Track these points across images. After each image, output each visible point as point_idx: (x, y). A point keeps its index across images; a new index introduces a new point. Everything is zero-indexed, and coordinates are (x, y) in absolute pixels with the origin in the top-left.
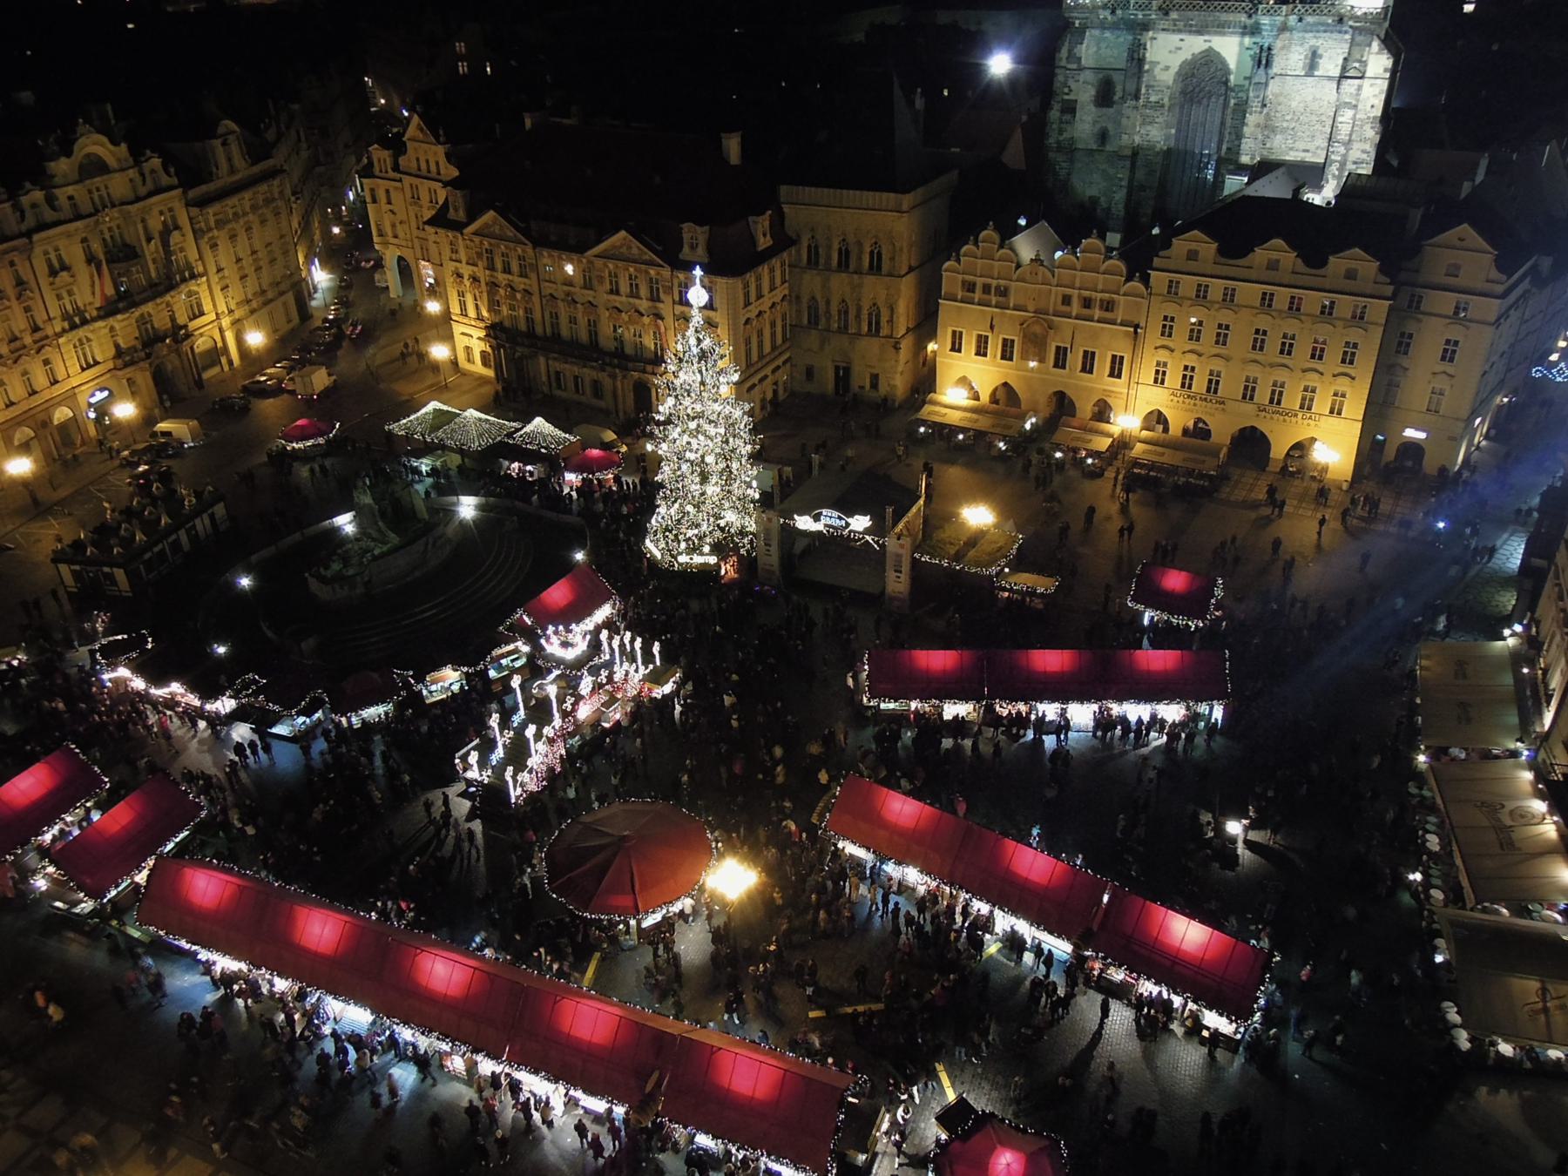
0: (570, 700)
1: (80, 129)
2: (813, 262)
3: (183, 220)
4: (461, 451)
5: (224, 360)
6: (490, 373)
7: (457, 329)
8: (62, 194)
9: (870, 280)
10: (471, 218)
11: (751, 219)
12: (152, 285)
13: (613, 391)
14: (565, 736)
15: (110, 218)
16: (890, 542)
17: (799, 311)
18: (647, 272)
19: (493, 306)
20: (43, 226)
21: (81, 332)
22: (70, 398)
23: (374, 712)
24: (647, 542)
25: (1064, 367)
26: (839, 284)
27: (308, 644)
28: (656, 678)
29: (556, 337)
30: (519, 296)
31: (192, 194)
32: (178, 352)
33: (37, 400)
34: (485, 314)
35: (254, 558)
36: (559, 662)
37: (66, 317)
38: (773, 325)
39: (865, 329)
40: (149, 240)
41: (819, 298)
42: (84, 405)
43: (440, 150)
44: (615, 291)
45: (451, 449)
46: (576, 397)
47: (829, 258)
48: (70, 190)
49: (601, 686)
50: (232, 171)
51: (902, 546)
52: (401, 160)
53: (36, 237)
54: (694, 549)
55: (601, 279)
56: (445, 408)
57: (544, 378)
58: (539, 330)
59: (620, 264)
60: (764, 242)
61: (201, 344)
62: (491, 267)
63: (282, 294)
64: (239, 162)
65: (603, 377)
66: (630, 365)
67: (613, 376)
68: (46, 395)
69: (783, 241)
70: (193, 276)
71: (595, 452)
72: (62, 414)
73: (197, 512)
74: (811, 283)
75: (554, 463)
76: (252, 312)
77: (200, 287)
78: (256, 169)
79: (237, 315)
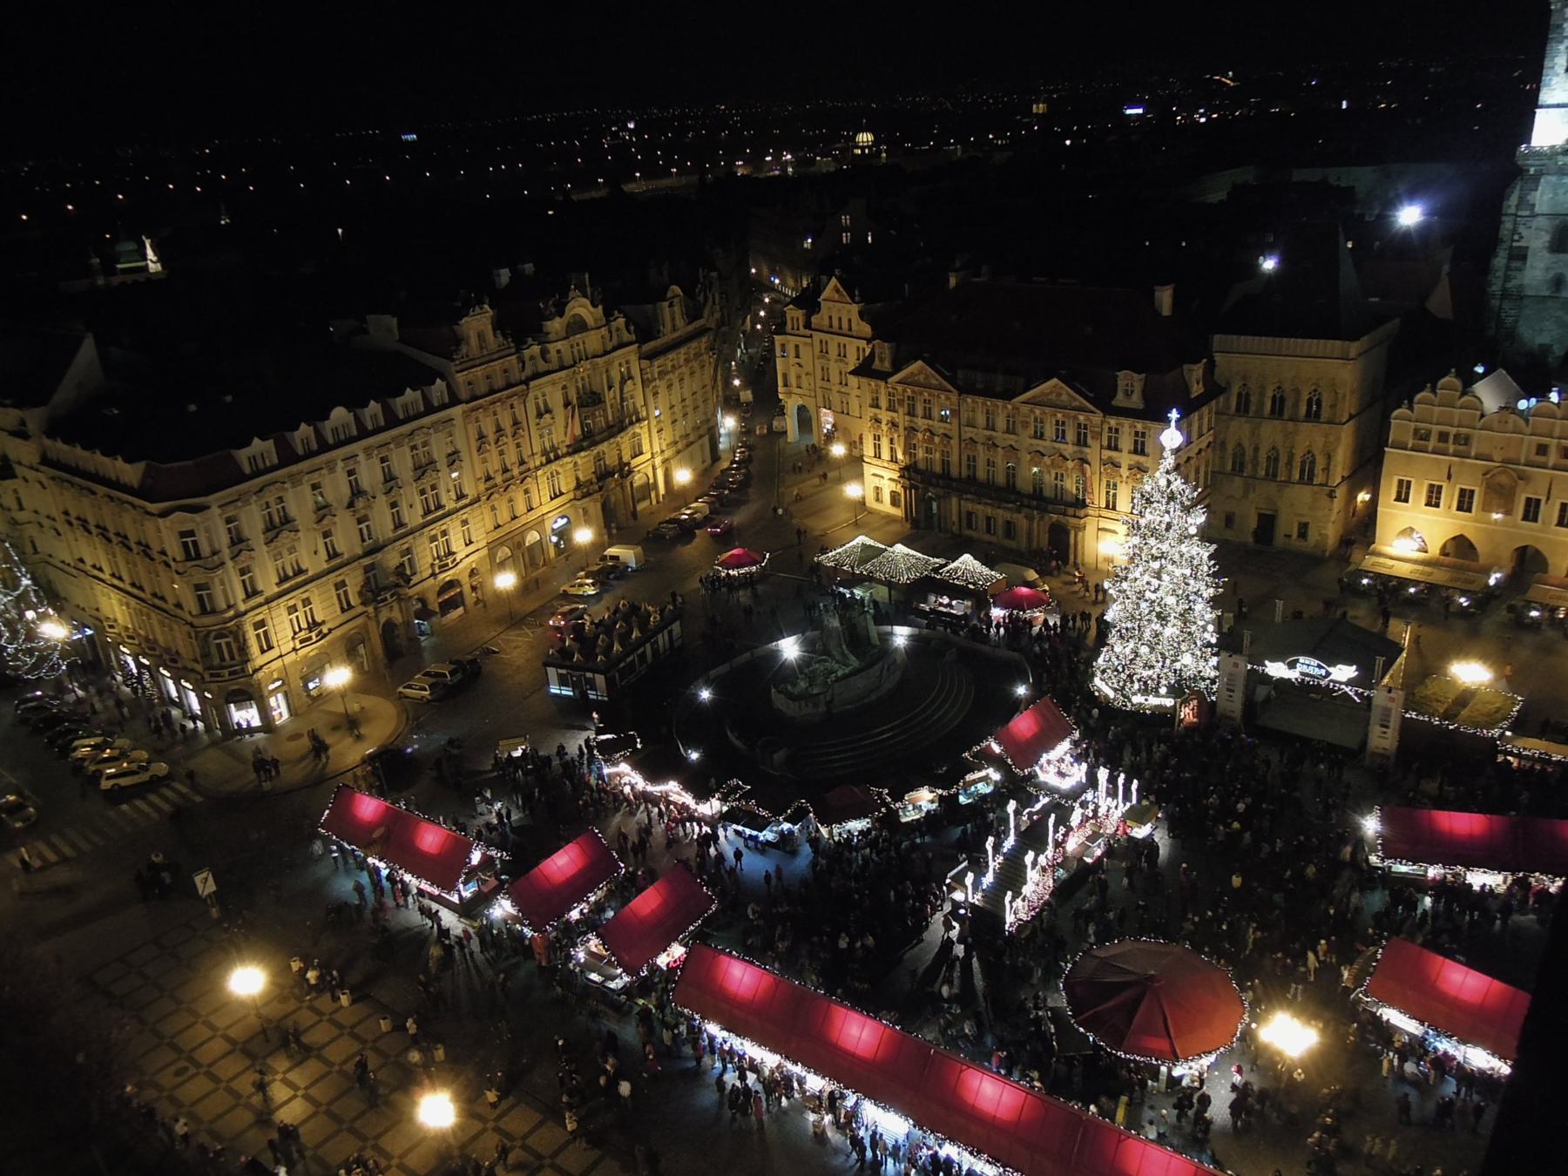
0: (1062, 830)
1: (571, 294)
2: (1243, 407)
3: (636, 372)
4: (889, 584)
5: (653, 495)
6: (898, 512)
7: (868, 470)
8: (552, 348)
9: (1306, 427)
10: (897, 368)
11: (1186, 367)
12: (610, 427)
13: (1041, 534)
14: (1054, 866)
15: (584, 368)
16: (1379, 696)
17: (1222, 458)
18: (1075, 418)
19: (909, 449)
20: (537, 375)
21: (553, 467)
22: (540, 522)
23: (856, 825)
24: (1097, 681)
25: (1535, 520)
26: (1271, 432)
27: (779, 756)
28: (1136, 815)
29: (972, 479)
30: (937, 439)
31: (647, 347)
32: (622, 487)
33: (517, 524)
34: (900, 456)
35: (713, 673)
36: (1051, 791)
37: (545, 453)
38: (1197, 472)
39: (1297, 476)
40: (610, 388)
41: (1246, 444)
42: (549, 531)
43: (855, 308)
44: (1040, 436)
45: (879, 582)
46: (987, 537)
47: (1261, 404)
48: (559, 345)
49: (1088, 819)
50: (674, 329)
51: (1392, 700)
52: (813, 319)
53: (532, 384)
54: (1145, 691)
55: (1025, 425)
56: (870, 542)
57: (955, 518)
58: (954, 472)
59: (1047, 410)
60: (1197, 390)
61: (638, 480)
62: (911, 413)
63: (701, 437)
64: (680, 322)
65: (1021, 521)
66: (1050, 507)
67: (1030, 518)
68: (523, 520)
69: (1214, 390)
70: (639, 420)
71: (1024, 590)
72: (532, 537)
73: (659, 629)
74: (1239, 430)
75: (980, 598)
76: (678, 452)
77: (641, 430)
78: (690, 328)
79: (667, 455)
